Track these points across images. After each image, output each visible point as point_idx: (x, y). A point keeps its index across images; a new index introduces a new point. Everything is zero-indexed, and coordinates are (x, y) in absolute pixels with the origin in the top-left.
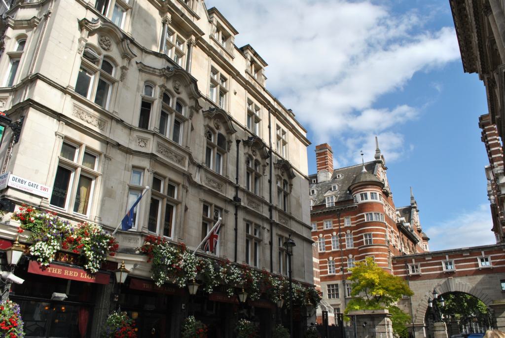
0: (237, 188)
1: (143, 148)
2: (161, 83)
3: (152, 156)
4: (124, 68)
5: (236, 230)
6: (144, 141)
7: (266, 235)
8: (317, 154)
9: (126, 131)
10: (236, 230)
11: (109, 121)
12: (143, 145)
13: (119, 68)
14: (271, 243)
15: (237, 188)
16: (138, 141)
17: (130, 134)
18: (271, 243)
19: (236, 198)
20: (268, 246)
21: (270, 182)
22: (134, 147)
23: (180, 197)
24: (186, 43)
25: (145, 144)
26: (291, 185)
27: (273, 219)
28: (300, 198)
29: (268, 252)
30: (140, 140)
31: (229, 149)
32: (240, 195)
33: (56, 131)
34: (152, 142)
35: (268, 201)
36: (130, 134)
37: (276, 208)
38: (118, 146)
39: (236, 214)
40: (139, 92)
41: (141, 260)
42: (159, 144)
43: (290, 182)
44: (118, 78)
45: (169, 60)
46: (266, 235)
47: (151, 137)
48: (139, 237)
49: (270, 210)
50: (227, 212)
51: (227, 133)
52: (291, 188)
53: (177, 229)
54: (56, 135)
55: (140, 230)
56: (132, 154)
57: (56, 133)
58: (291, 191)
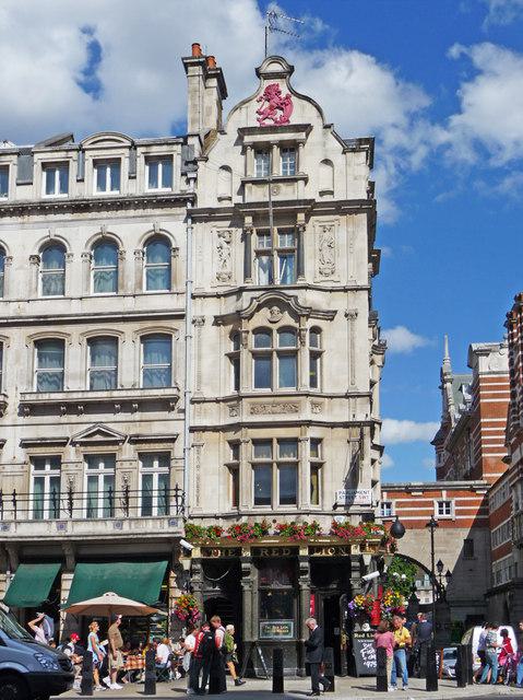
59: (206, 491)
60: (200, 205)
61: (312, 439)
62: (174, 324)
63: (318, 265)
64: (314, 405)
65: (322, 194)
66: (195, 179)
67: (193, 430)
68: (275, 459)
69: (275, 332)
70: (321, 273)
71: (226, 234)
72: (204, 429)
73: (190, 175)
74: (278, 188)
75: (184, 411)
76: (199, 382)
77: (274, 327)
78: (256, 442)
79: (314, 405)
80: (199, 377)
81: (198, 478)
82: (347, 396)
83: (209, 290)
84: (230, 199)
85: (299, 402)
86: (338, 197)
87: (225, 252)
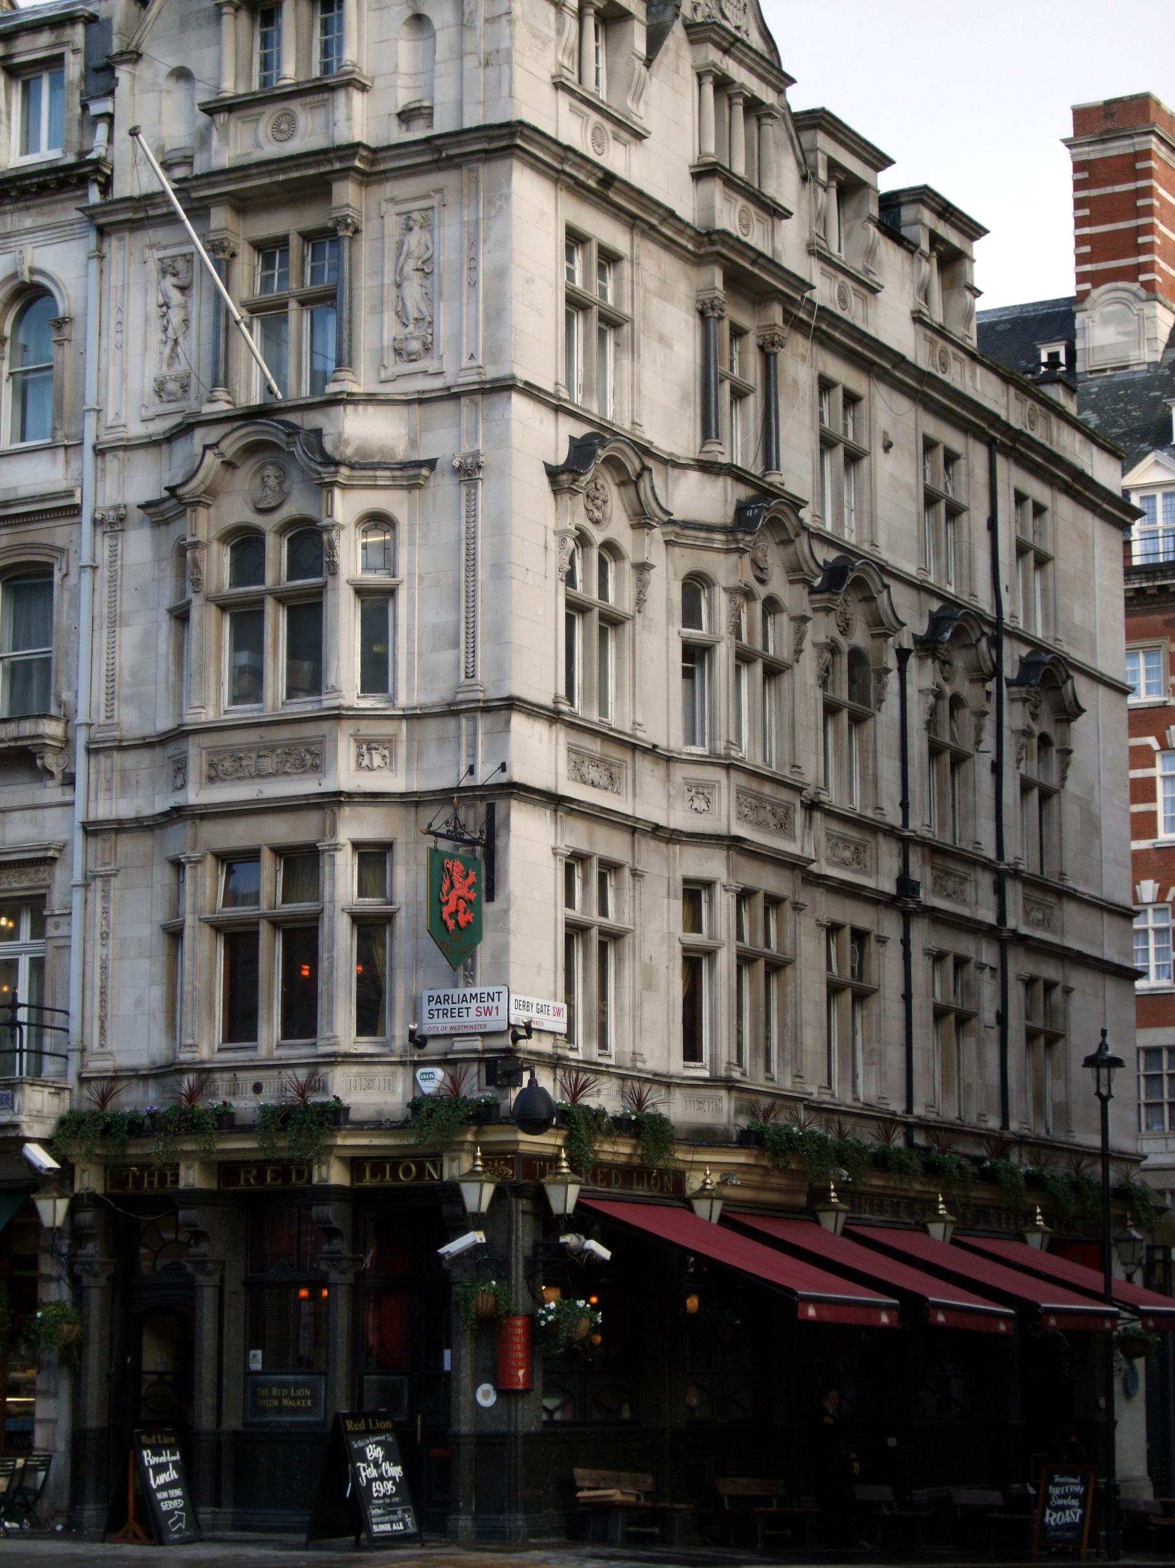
0: (905, 842)
1: (704, 816)
2: (733, 582)
3: (733, 844)
4: (642, 568)
5: (907, 997)
6: (700, 789)
7: (988, 991)
8: (1078, 167)
9: (660, 771)
10: (907, 997)
11: (627, 756)
12: (704, 806)
13: (627, 565)
14: (1002, 1018)
15: (905, 842)
16: (688, 796)
17: (668, 775)
18: (1002, 1018)
19: (906, 884)
20: (994, 1033)
21: (997, 768)
22: (680, 818)
23: (788, 942)
24: (751, 341)
25: (708, 801)
26: (1066, 752)
27: (1011, 923)
28: (1096, 793)
29: (992, 1053)
30: (693, 793)
31: (880, 701)
32: (919, 871)
33: (553, 844)
34: (724, 792)
35: (991, 854)
36: (668, 775)
37: (1016, 874)
38: (657, 831)
39: (906, 942)
40: (673, 624)
41: (742, 1159)
42: (740, 791)
43: (1065, 740)
44: (627, 606)
45: (738, 475)
46: (988, 991)
47: (719, 775)
48: (723, 1093)
49: (999, 890)
50: (882, 941)
51: (874, 636)
52: (1065, 765)
53: (788, 1046)
54: (555, 854)
55: (722, 1073)
56: (679, 842)
57: (553, 849)
58: (1063, 779)
59: (123, 1004)
60: (124, 187)
61: (356, 845)
62: (58, 533)
63: (391, 328)
64: (367, 745)
65: (406, 116)
66: (109, 117)
67: (91, 830)
68: (264, 907)
69: (270, 540)
70: (398, 352)
71: (180, 265)
72: (120, 827)
73: (96, 108)
74: (292, 120)
75: (69, 781)
76: (111, 695)
77: (267, 524)
78: (231, 860)
79: (367, 745)
80: (111, 678)
81: (104, 968)
82: (451, 711)
83: (137, 430)
84: (188, 161)
85: (321, 740)
86: (443, 123)
87: (176, 316)
